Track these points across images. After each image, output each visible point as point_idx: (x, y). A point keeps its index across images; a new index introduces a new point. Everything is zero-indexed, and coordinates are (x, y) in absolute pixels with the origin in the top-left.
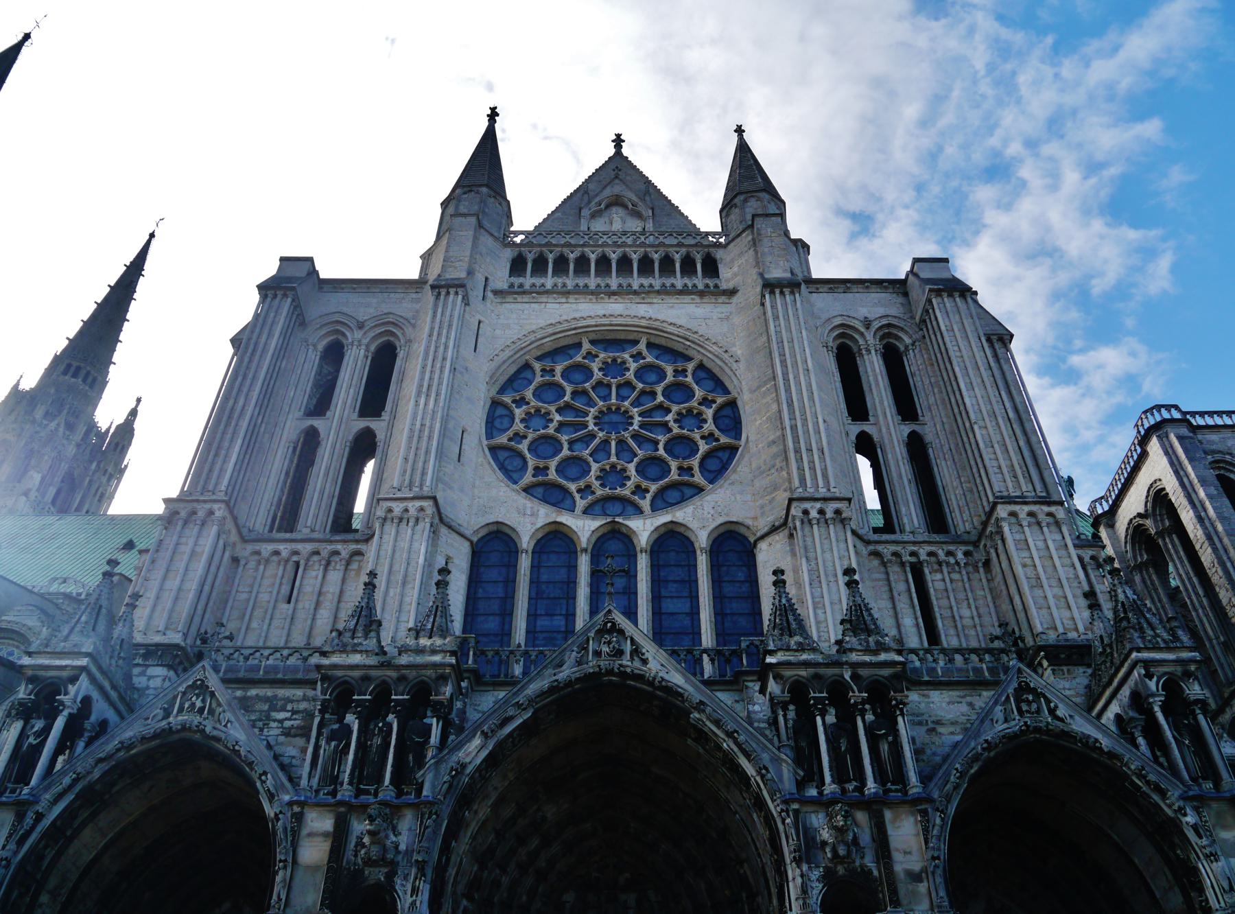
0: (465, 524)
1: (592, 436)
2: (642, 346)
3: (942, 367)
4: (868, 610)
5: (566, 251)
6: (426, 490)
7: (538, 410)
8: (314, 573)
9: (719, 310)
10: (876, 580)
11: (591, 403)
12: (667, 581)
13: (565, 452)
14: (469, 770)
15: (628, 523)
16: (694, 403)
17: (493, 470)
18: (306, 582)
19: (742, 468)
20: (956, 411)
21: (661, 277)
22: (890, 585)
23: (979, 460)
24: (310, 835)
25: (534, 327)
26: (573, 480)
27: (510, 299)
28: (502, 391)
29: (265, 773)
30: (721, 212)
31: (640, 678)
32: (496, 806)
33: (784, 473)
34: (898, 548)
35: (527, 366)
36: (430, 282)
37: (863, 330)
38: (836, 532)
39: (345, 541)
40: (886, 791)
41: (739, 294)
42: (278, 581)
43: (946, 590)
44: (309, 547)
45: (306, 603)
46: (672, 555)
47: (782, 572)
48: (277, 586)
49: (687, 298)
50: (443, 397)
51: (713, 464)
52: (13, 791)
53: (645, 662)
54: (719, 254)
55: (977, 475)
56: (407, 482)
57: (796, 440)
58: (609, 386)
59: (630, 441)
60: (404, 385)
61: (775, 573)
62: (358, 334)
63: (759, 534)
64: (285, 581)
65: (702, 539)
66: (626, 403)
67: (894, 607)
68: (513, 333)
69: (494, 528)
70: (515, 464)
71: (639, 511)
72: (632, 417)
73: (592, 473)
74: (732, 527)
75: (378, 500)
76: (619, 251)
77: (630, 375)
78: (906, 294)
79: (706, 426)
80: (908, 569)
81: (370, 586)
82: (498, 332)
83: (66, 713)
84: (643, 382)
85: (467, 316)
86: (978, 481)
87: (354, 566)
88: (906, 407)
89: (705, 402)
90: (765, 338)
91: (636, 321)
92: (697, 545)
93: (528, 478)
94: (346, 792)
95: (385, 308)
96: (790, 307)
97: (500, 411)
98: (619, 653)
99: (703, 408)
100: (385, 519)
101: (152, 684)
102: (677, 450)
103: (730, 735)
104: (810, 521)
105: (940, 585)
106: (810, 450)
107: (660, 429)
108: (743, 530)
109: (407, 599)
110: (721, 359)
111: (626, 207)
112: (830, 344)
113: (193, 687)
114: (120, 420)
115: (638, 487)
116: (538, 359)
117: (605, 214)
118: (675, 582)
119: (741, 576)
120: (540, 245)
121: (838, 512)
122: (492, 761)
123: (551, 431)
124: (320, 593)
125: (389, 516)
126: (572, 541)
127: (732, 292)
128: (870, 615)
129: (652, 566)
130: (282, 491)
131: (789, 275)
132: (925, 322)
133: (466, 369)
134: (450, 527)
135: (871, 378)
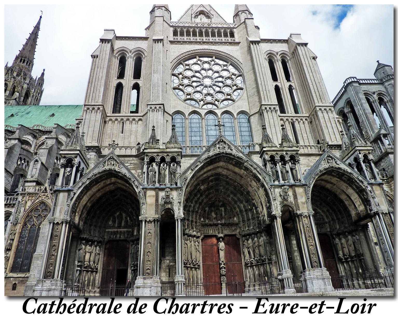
14: (189, 179)
18: (126, 128)
24: (149, 196)
25: (183, 53)
29: (135, 181)
30: (234, 17)
31: (231, 154)
32: (191, 187)
40: (295, 182)
52: (66, 187)
53: (232, 150)
54: (235, 30)
55: (309, 98)
59: (213, 87)
61: (263, 126)
62: (130, 54)
80: (291, 124)
81: (153, 130)
82: (172, 54)
83: (75, 166)
86: (309, 99)
94: (157, 185)
98: (225, 147)
101: (92, 157)
103: (255, 169)
113: (109, 159)
114: (39, 76)
117: (199, 16)
121: (274, 108)
122: (193, 177)
127: (239, 43)
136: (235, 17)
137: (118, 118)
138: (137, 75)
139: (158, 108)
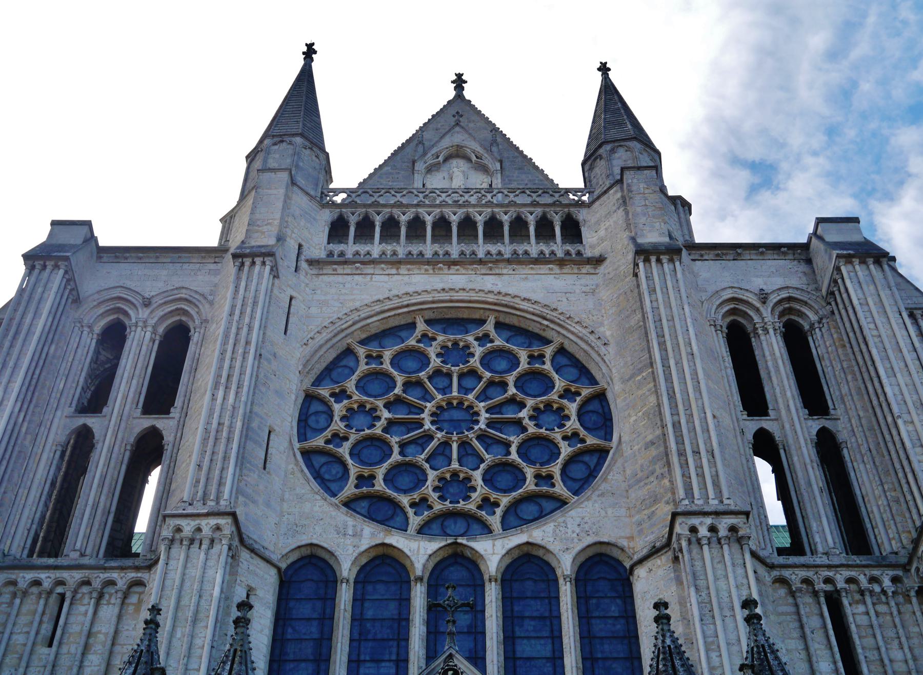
0: (272, 548)
1: (429, 437)
2: (489, 327)
3: (856, 349)
4: (774, 652)
5: (396, 212)
6: (224, 505)
7: (362, 406)
8: (83, 609)
9: (583, 281)
10: (782, 614)
11: (427, 396)
12: (523, 618)
13: (396, 457)
15: (472, 544)
16: (554, 396)
17: (308, 481)
18: (72, 619)
19: (613, 475)
20: (875, 402)
21: (511, 242)
22: (800, 620)
23: (905, 463)
25: (358, 304)
26: (405, 492)
27: (328, 270)
28: (318, 382)
30: (583, 164)
33: (666, 482)
34: (810, 574)
35: (349, 352)
36: (232, 250)
37: (758, 305)
38: (731, 554)
39: (122, 568)
41: (608, 261)
42: (37, 618)
43: (872, 626)
44: (78, 575)
45: (72, 648)
46: (529, 585)
47: (666, 605)
48: (36, 624)
49: (544, 269)
50: (245, 389)
51: (578, 471)
54: (581, 215)
55: (903, 481)
56: (200, 494)
57: (680, 441)
58: (449, 375)
59: (476, 444)
60: (198, 376)
61: (657, 606)
62: (144, 313)
63: (636, 558)
64: (45, 619)
65: (566, 565)
66: (470, 397)
67: (807, 648)
68: (334, 311)
69: (307, 552)
70: (334, 472)
71: (487, 530)
72: (477, 414)
73: (429, 483)
74: (603, 550)
75: (165, 517)
76: (461, 212)
77: (475, 362)
78: (809, 261)
79: (568, 424)
80: (822, 600)
81: (152, 625)
82: (314, 310)
84: (491, 371)
85: (276, 291)
87: (133, 599)
88: (814, 398)
89: (567, 394)
90: (640, 316)
91: (481, 297)
92: (559, 572)
93: (350, 490)
95: (176, 282)
96: (668, 277)
97: (316, 407)
99: (565, 401)
100: (172, 541)
102: (535, 452)
104: (699, 541)
105: (863, 620)
106: (697, 452)
107: (512, 429)
108: (616, 553)
109: (198, 642)
110: (587, 342)
111: (469, 160)
112: (719, 322)
115: (486, 500)
116: (363, 342)
117: (445, 168)
118: (532, 618)
119: (614, 610)
120: (365, 206)
121: (733, 529)
123: (378, 431)
124: (89, 635)
125: (178, 536)
126: (403, 567)
127: (599, 261)
128: (777, 658)
129: (504, 598)
130: (46, 506)
131: (667, 239)
132: (833, 294)
133: (275, 355)
134: (253, 551)
135: (770, 364)
136: (587, 167)
137: (42, 575)
138: (162, 392)
139: (206, 531)
